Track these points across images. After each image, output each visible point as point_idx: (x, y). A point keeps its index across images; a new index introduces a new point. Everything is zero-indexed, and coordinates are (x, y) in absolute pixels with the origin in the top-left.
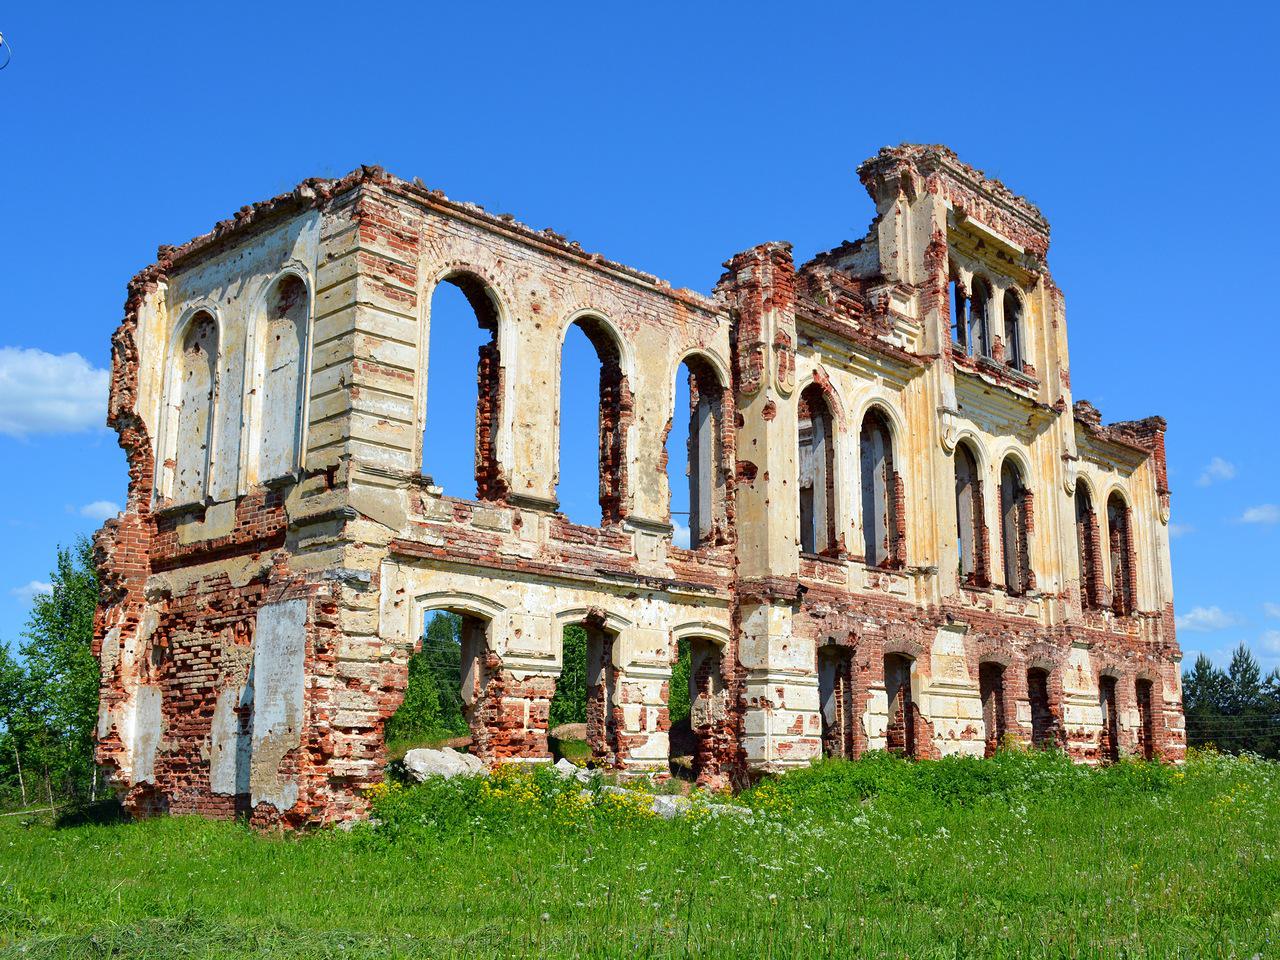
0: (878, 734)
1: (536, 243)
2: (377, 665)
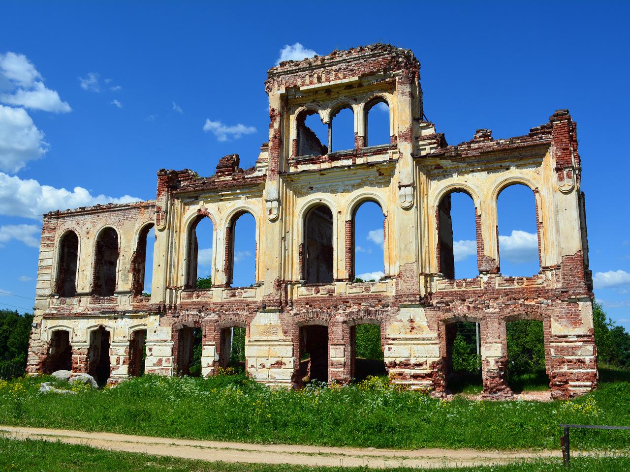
0: (206, 365)
1: (88, 212)
2: (40, 348)
